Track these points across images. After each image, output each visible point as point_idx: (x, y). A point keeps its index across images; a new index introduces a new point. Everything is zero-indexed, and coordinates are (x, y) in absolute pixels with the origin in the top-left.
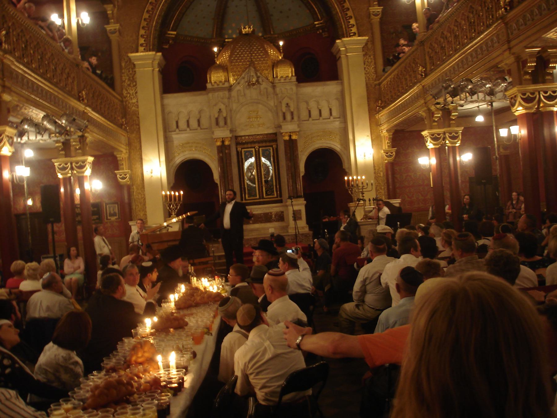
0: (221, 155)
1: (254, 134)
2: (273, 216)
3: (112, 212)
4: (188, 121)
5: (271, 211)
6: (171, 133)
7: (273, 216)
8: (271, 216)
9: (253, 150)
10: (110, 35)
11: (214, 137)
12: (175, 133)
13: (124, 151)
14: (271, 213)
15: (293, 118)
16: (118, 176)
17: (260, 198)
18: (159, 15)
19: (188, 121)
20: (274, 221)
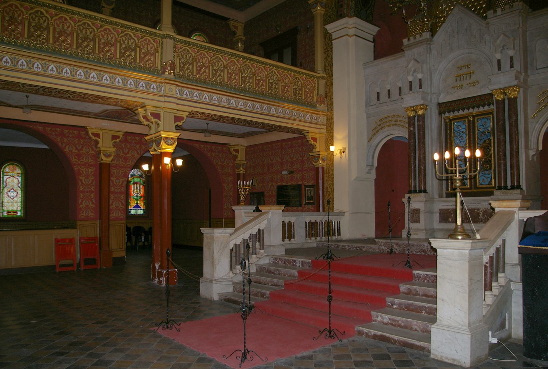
0: (412, 129)
1: (463, 98)
2: (481, 215)
3: (309, 196)
4: (389, 91)
5: (479, 206)
6: (371, 107)
7: (481, 215)
8: (478, 214)
9: (467, 119)
11: (404, 106)
12: (375, 106)
14: (478, 210)
15: (512, 66)
17: (471, 188)
19: (389, 91)
20: (482, 221)
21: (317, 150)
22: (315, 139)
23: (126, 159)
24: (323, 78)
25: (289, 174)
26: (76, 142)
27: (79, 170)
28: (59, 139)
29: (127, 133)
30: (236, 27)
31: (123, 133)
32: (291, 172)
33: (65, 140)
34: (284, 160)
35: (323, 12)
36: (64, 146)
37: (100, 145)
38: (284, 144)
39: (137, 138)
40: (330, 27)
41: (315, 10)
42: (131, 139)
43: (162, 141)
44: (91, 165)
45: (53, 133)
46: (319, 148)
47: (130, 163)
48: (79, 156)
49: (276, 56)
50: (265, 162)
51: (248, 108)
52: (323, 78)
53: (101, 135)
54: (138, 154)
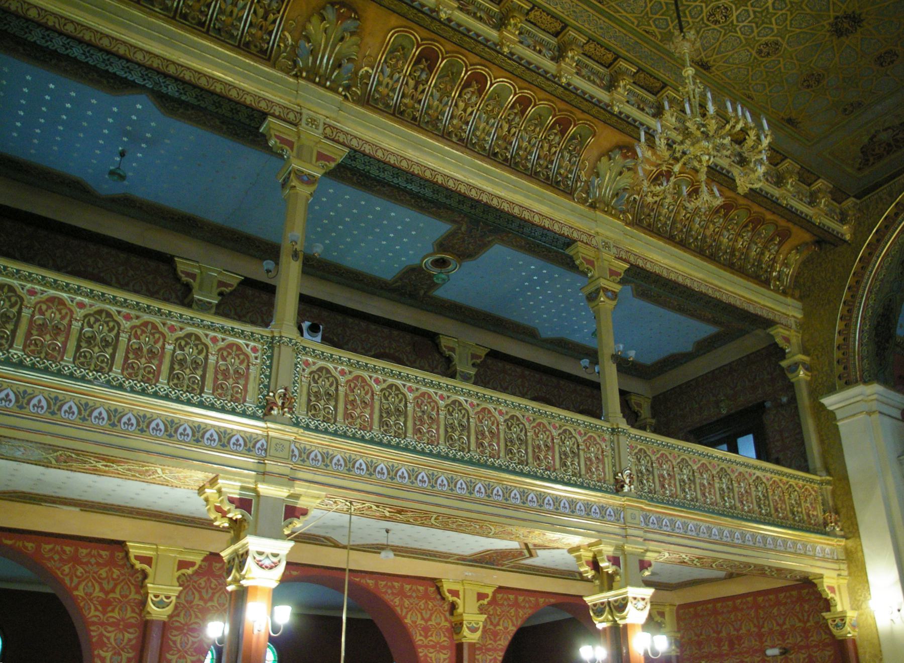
10: (790, 376)
13: (834, 574)
16: (830, 622)
18: (863, 318)
21: (839, 608)
22: (832, 589)
23: (495, 634)
24: (828, 483)
25: (782, 654)
26: (422, 607)
27: (426, 655)
28: (397, 601)
29: (501, 589)
30: (639, 405)
31: (493, 590)
32: (785, 652)
33: (407, 603)
34: (765, 629)
35: (809, 378)
36: (404, 614)
37: (460, 610)
38: (760, 599)
39: (512, 597)
40: (830, 402)
41: (794, 375)
42: (502, 598)
43: (629, 604)
44: (443, 648)
45: (389, 591)
46: (842, 603)
47: (501, 642)
48: (426, 630)
49: (725, 446)
50: (724, 634)
51: (736, 541)
52: (828, 483)
53: (461, 593)
54: (513, 625)
